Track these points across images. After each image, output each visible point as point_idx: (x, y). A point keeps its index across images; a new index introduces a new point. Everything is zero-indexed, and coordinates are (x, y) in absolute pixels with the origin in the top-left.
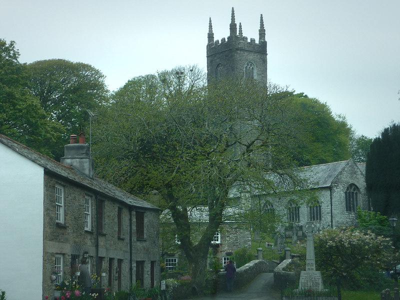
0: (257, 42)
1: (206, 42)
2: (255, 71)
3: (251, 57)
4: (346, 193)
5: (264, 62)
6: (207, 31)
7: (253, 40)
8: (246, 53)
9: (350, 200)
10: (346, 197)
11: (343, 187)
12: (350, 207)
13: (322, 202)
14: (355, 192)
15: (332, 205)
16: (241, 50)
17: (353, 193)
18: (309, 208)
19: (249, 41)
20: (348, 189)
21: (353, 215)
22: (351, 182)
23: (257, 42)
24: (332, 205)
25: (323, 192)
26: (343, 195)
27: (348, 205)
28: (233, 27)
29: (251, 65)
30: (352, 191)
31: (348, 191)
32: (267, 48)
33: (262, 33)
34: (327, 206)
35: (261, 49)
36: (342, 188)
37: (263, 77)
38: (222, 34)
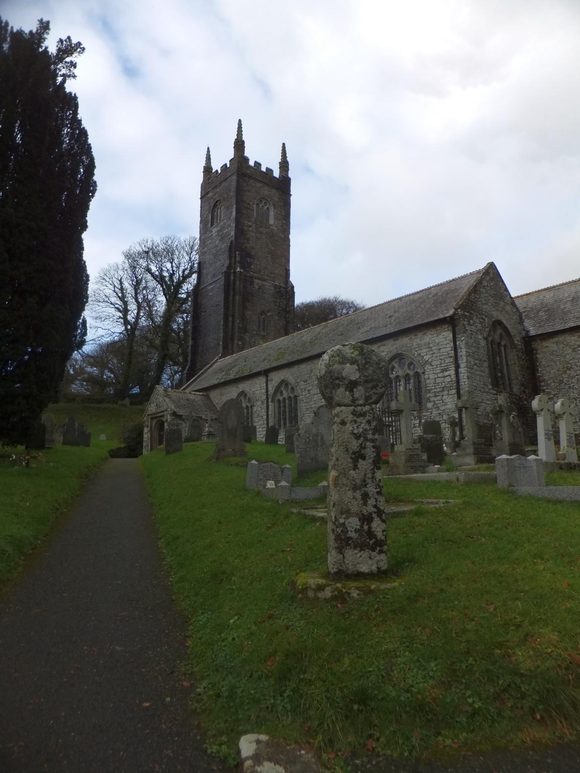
0: (276, 174)
1: (200, 178)
2: (272, 214)
3: (265, 191)
6: (203, 163)
7: (269, 171)
8: (258, 185)
11: (481, 323)
13: (427, 362)
14: (503, 343)
15: (457, 367)
16: (250, 177)
17: (499, 344)
19: (263, 169)
20: (489, 336)
22: (496, 315)
23: (276, 174)
24: (457, 367)
25: (429, 337)
26: (483, 343)
28: (239, 145)
30: (497, 338)
31: (490, 339)
32: (291, 188)
33: (284, 165)
34: (443, 371)
36: (479, 326)
38: (223, 157)
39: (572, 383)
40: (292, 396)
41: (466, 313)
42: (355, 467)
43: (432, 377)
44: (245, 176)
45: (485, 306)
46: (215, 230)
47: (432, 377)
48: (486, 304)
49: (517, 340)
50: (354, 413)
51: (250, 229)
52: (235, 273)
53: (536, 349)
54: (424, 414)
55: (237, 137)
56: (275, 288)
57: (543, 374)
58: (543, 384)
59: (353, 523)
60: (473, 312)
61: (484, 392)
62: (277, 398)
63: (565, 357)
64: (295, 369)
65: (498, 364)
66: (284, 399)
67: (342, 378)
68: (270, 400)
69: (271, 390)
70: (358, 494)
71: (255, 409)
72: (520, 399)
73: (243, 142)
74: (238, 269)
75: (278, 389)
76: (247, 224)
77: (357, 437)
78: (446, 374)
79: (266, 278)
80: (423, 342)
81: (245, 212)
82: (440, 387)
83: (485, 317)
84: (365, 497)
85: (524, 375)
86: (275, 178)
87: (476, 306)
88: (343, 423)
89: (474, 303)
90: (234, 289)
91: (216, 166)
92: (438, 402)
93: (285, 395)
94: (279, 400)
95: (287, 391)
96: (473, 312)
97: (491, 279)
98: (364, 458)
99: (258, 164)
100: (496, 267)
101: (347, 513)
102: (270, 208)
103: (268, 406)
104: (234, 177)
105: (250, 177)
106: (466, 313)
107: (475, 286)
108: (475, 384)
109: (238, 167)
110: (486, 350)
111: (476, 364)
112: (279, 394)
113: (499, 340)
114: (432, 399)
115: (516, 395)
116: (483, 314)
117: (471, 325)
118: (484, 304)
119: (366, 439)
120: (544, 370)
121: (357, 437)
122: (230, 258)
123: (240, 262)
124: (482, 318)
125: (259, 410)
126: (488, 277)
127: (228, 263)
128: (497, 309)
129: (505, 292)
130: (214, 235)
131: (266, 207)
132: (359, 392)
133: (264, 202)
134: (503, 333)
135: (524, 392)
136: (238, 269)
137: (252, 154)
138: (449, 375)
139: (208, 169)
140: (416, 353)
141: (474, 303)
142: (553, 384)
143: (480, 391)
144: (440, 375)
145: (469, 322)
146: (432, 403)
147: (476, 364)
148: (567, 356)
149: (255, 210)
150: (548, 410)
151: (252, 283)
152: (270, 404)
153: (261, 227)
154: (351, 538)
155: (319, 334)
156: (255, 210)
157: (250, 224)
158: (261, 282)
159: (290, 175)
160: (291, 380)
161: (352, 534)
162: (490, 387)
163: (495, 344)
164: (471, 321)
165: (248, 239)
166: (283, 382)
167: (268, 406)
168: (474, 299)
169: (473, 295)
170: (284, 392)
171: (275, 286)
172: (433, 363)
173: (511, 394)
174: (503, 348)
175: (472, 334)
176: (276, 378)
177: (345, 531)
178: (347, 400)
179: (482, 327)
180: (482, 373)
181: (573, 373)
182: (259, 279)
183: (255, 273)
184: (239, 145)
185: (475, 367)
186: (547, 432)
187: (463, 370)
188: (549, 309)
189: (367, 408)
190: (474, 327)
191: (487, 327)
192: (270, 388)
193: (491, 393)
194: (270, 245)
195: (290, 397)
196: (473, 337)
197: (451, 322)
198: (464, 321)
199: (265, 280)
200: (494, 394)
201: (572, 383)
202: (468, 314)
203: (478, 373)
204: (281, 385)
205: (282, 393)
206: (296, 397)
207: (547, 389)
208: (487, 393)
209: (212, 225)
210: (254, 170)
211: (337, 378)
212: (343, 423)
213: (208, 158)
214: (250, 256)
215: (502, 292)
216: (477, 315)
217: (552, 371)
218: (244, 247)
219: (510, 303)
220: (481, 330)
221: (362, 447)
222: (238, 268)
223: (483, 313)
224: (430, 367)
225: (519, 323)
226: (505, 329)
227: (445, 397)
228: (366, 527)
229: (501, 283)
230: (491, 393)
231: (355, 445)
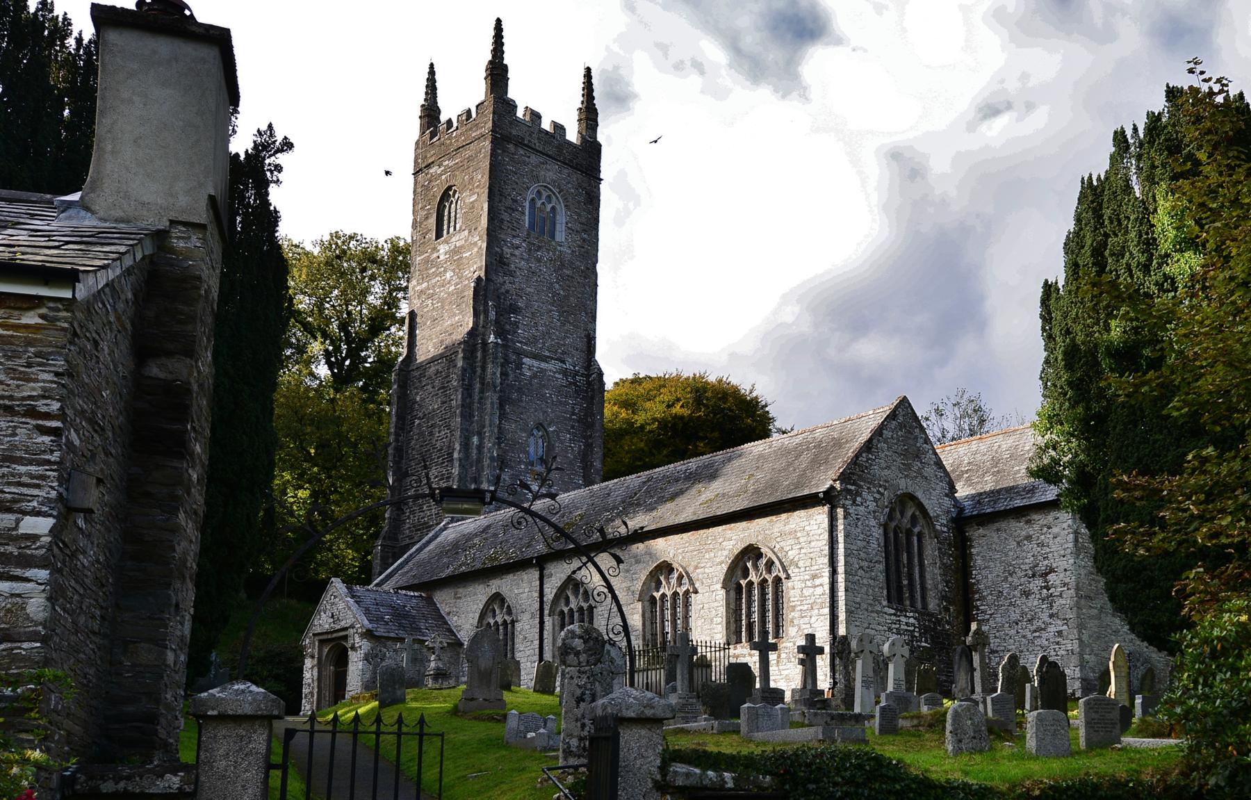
0: (572, 135)
2: (562, 219)
3: (551, 172)
4: (885, 526)
7: (559, 128)
8: (534, 159)
9: (898, 561)
10: (886, 546)
11: (875, 500)
12: (900, 588)
14: (916, 530)
16: (520, 143)
17: (909, 533)
18: (733, 593)
19: (546, 125)
20: (891, 517)
21: (909, 620)
22: (904, 485)
23: (572, 135)
26: (877, 533)
27: (893, 577)
29: (549, 197)
30: (906, 522)
31: (893, 525)
32: (602, 164)
33: (589, 115)
34: (814, 577)
36: (872, 506)
37: (584, 240)
39: (1014, 596)
40: (585, 606)
41: (849, 487)
42: (578, 707)
43: (799, 585)
44: (509, 142)
45: (886, 472)
46: (443, 248)
47: (799, 585)
48: (888, 467)
49: (941, 525)
50: (579, 671)
51: (517, 252)
52: (485, 344)
53: (970, 540)
54: (784, 645)
55: (493, 56)
57: (978, 581)
58: (977, 596)
59: (574, 742)
60: (862, 483)
61: (872, 612)
62: (558, 609)
63: (1007, 555)
65: (904, 565)
66: (571, 610)
67: (572, 649)
68: (546, 612)
69: (550, 594)
70: (579, 724)
71: (518, 626)
72: (939, 622)
74: (492, 338)
75: (562, 590)
76: (511, 242)
77: (580, 687)
78: (818, 582)
79: (547, 353)
80: (787, 528)
81: (506, 216)
82: (807, 602)
83: (885, 490)
84: (583, 726)
85: (947, 582)
86: (570, 143)
87: (869, 473)
88: (572, 678)
89: (866, 468)
90: (482, 379)
92: (804, 626)
93: (573, 605)
94: (562, 612)
95: (577, 597)
96: (862, 483)
97: (901, 426)
98: (584, 701)
99: (536, 117)
100: (910, 404)
101: (571, 736)
102: (558, 207)
103: (542, 623)
104: (487, 144)
105: (520, 143)
106: (849, 487)
107: (870, 441)
108: (858, 600)
109: (494, 122)
110: (882, 544)
111: (861, 568)
112: (562, 602)
113: (909, 526)
114: (796, 622)
115: (932, 615)
116: (880, 486)
117: (858, 505)
118: (882, 469)
119: (586, 689)
120: (979, 574)
121: (580, 687)
122: (476, 314)
123: (497, 322)
124: (879, 492)
125: (526, 627)
126: (894, 422)
127: (471, 325)
128: (906, 476)
129: (925, 445)
130: (442, 257)
131: (551, 205)
132: (583, 657)
133: (545, 194)
134: (917, 513)
135: (947, 609)
136: (492, 338)
137: (521, 93)
138: (821, 585)
140: (778, 546)
141: (866, 468)
142: (990, 597)
143: (867, 610)
144: (809, 584)
145: (854, 501)
146: (795, 629)
147: (861, 568)
148: (1010, 553)
149: (527, 213)
150: (871, 652)
151: (519, 365)
152: (546, 618)
153: (539, 248)
154: (572, 751)
155: (636, 494)
156: (527, 213)
157: (516, 242)
158: (536, 363)
159: (603, 135)
161: (574, 749)
162: (885, 603)
163: (901, 532)
164: (859, 499)
165: (512, 274)
167: (542, 623)
168: (867, 461)
169: (864, 455)
170: (572, 598)
171: (565, 372)
172: (801, 564)
173: (924, 613)
174: (915, 538)
175: (857, 519)
176: (558, 573)
177: (569, 747)
178: (576, 663)
179: (877, 506)
180: (871, 582)
181: (1016, 582)
182: (535, 357)
183: (526, 344)
185: (860, 572)
186: (865, 679)
187: (841, 578)
188: (998, 472)
189: (587, 668)
190: (862, 508)
191: (887, 507)
192: (547, 590)
193: (886, 613)
194: (557, 286)
195: (581, 609)
196: (859, 523)
197: (829, 499)
198: (847, 499)
199: (545, 359)
200: (891, 615)
201: (1014, 596)
202: (853, 488)
203: (865, 581)
204: (566, 586)
205: (567, 602)
206: (591, 608)
207: (982, 605)
208: (878, 612)
209: (439, 235)
210: (525, 128)
211: (569, 648)
212: (572, 678)
214: (515, 309)
215: (918, 445)
216: (869, 488)
217: (989, 576)
218: (503, 290)
219: (932, 463)
220: (874, 512)
221: (583, 694)
222: (492, 336)
223: (881, 483)
224: (797, 570)
225: (947, 495)
226: (920, 506)
227: (813, 619)
228: (582, 745)
229: (917, 430)
230: (886, 613)
231: (578, 692)
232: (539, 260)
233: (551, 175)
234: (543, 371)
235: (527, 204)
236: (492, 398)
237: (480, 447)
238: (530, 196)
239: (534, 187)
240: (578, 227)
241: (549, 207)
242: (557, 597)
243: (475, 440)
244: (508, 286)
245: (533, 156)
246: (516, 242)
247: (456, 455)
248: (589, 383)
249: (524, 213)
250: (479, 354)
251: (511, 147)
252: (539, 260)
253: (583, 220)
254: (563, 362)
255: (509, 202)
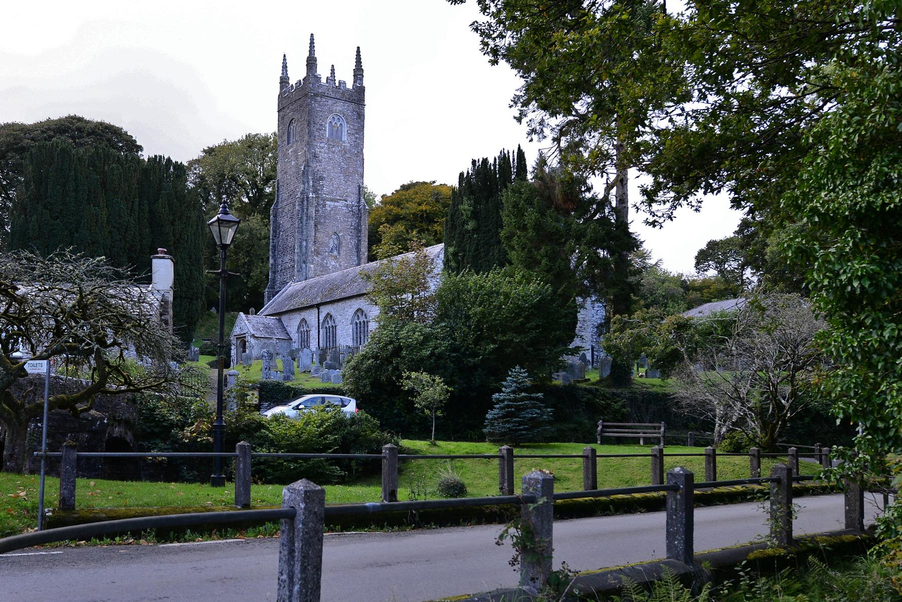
0: (350, 85)
2: (345, 129)
3: (339, 106)
5: (361, 116)
8: (330, 102)
16: (323, 95)
23: (350, 85)
28: (311, 62)
35: (357, 96)
37: (356, 138)
51: (322, 150)
52: (308, 198)
56: (347, 207)
64: (335, 305)
69: (321, 321)
73: (315, 60)
75: (326, 317)
81: (317, 134)
91: (293, 81)
105: (323, 95)
139: (284, 81)
151: (324, 206)
157: (322, 145)
158: (332, 203)
160: (333, 313)
166: (328, 314)
171: (347, 206)
176: (325, 310)
184: (311, 62)
199: (337, 201)
206: (336, 326)
213: (285, 67)
214: (322, 178)
232: (333, 152)
233: (339, 108)
234: (336, 207)
235: (327, 126)
236: (312, 223)
237: (306, 246)
238: (328, 121)
239: (331, 116)
240: (353, 132)
241: (339, 124)
242: (324, 321)
243: (304, 243)
244: (318, 168)
245: (330, 101)
246: (322, 145)
247: (296, 251)
248: (359, 210)
249: (325, 130)
250: (305, 203)
251: (319, 98)
252: (333, 152)
253: (356, 128)
254: (346, 201)
255: (318, 126)
